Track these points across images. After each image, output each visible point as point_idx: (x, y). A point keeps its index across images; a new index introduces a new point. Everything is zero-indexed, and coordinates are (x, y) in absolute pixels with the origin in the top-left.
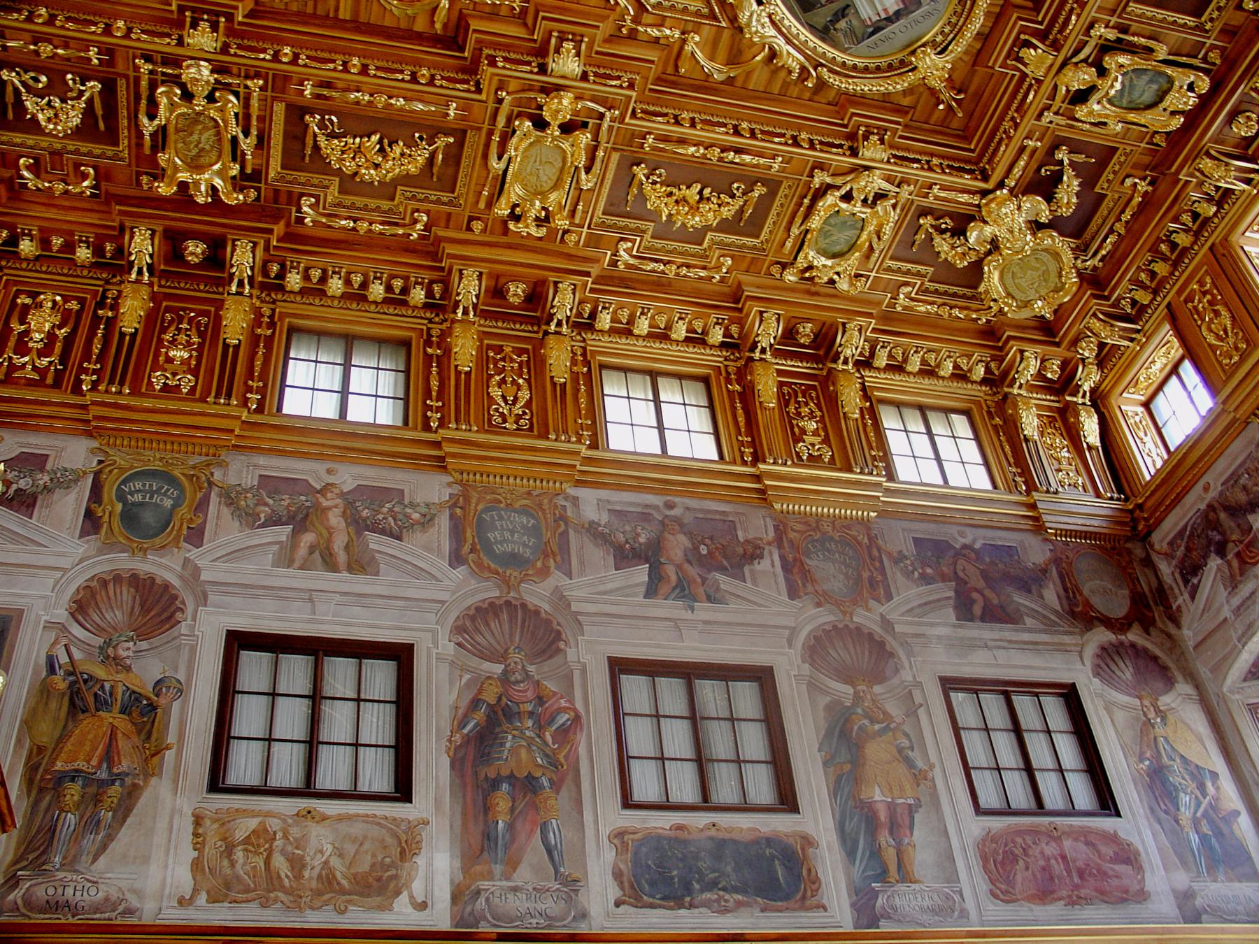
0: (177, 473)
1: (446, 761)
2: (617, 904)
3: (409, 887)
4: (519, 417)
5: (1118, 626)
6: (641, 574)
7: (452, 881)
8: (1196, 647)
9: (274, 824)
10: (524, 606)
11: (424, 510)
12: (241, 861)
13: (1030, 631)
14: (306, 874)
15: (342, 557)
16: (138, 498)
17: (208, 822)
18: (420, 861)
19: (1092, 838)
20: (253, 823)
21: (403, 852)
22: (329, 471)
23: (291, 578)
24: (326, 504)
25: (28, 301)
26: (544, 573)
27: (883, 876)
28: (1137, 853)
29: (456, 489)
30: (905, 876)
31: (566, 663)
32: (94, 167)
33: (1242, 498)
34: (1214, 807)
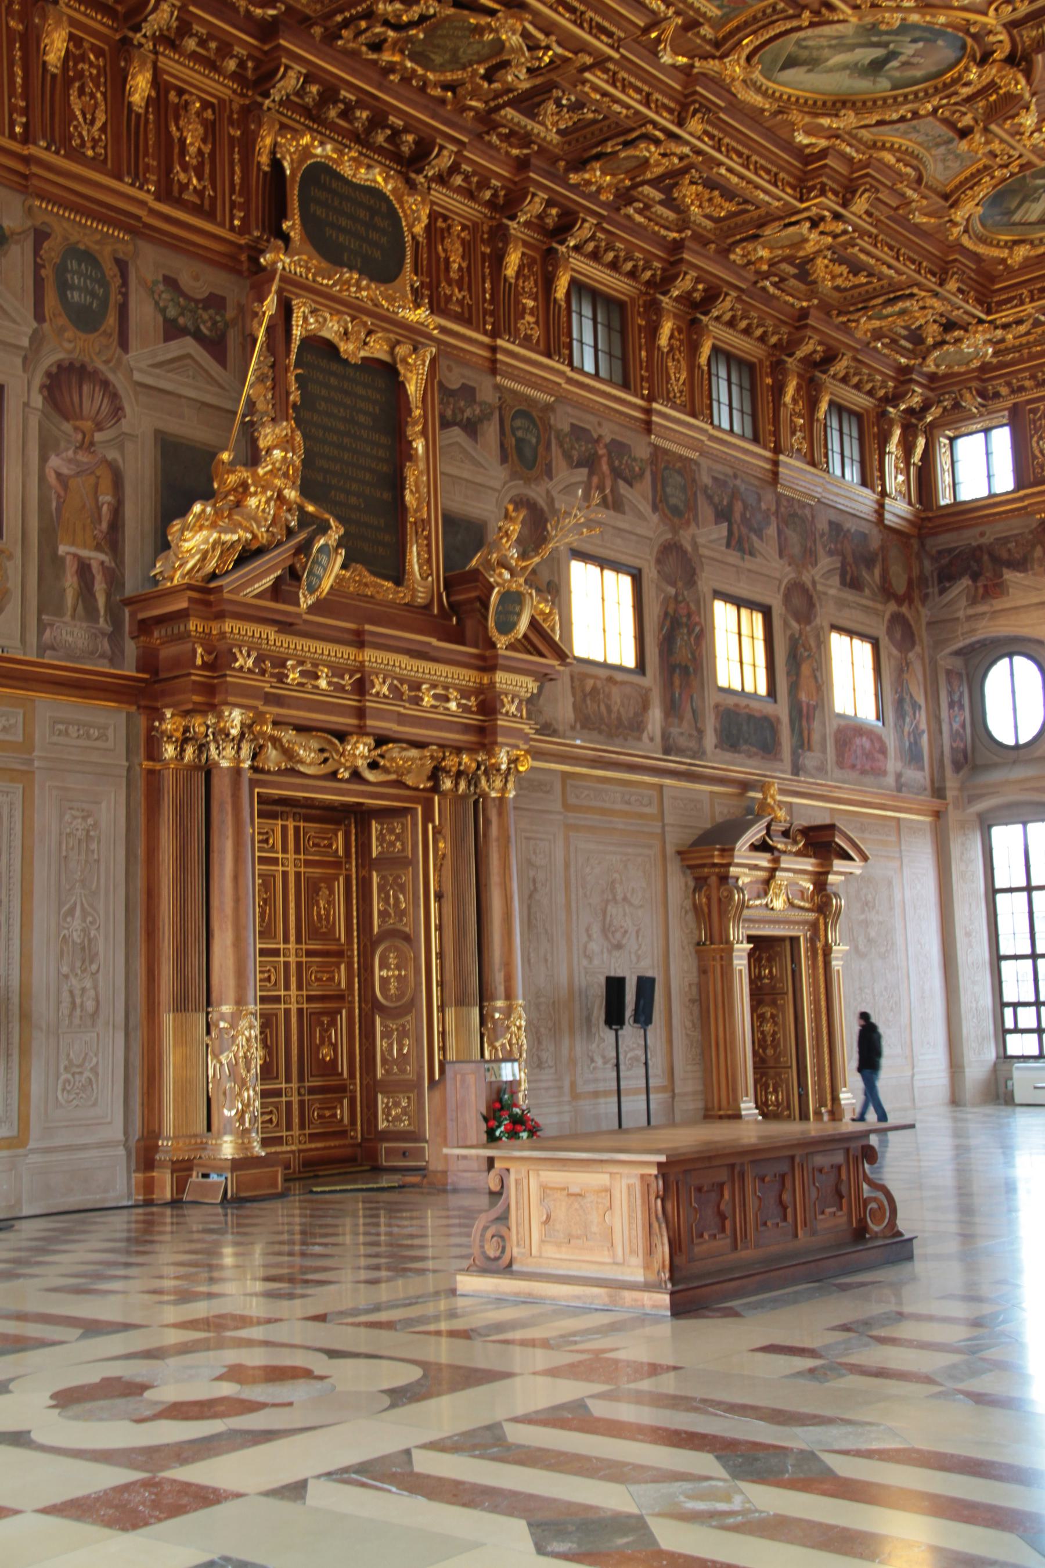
0: (534, 414)
9: (599, 684)
13: (867, 598)
16: (519, 434)
18: (650, 712)
25: (444, 225)
26: (688, 523)
27: (802, 746)
30: (810, 749)
32: (539, 146)
33: (1005, 555)
34: (917, 727)
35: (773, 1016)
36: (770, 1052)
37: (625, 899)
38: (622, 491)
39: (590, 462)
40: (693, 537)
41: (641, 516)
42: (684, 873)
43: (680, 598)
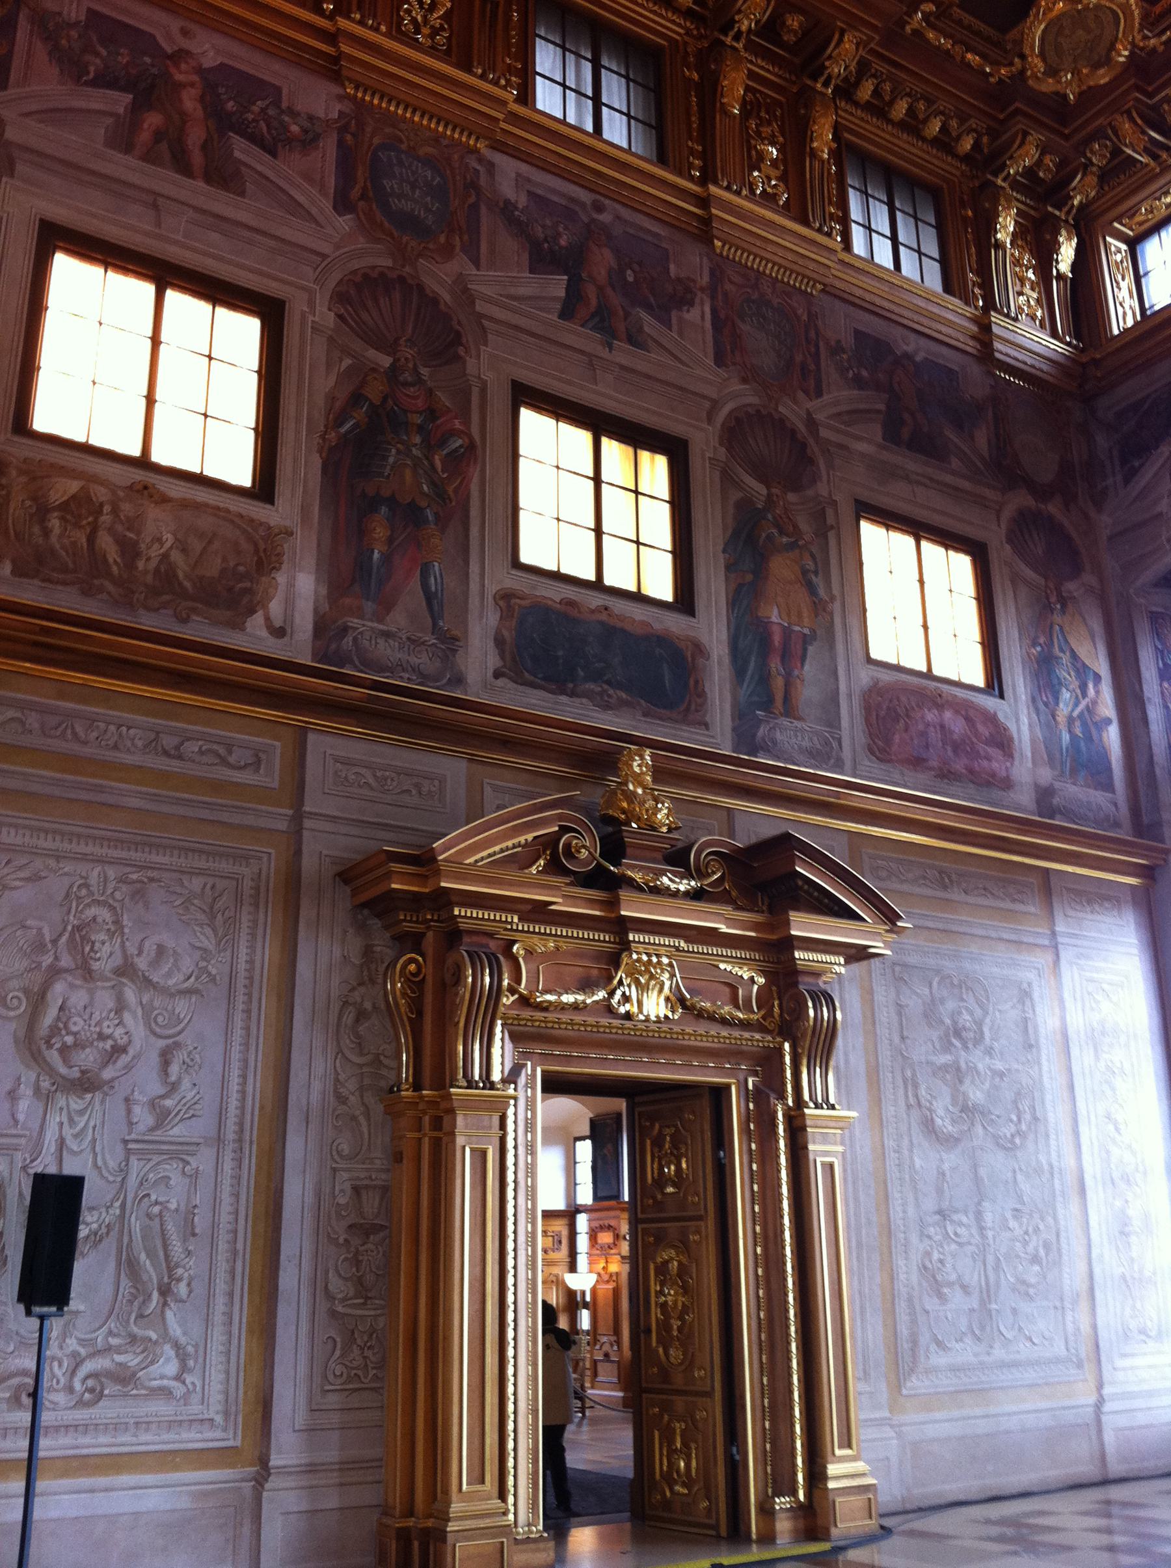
1: (317, 461)
2: (497, 675)
3: (265, 607)
4: (435, 31)
5: (1042, 493)
6: (557, 285)
7: (316, 611)
8: (1110, 538)
9: (101, 494)
10: (421, 288)
11: (307, 124)
12: (57, 531)
13: (954, 473)
14: (141, 565)
15: (197, 159)
17: (14, 473)
18: (281, 578)
19: (972, 713)
20: (74, 486)
21: (260, 564)
22: (185, 32)
23: (125, 167)
24: (179, 77)
26: (447, 252)
27: (767, 704)
28: (1011, 739)
29: (347, 107)
30: (790, 710)
31: (465, 375)
34: (1091, 710)
35: (683, 1270)
36: (675, 1354)
37: (126, 970)
38: (237, 154)
39: (148, 88)
40: (460, 279)
41: (295, 208)
42: (362, 928)
43: (407, 376)
